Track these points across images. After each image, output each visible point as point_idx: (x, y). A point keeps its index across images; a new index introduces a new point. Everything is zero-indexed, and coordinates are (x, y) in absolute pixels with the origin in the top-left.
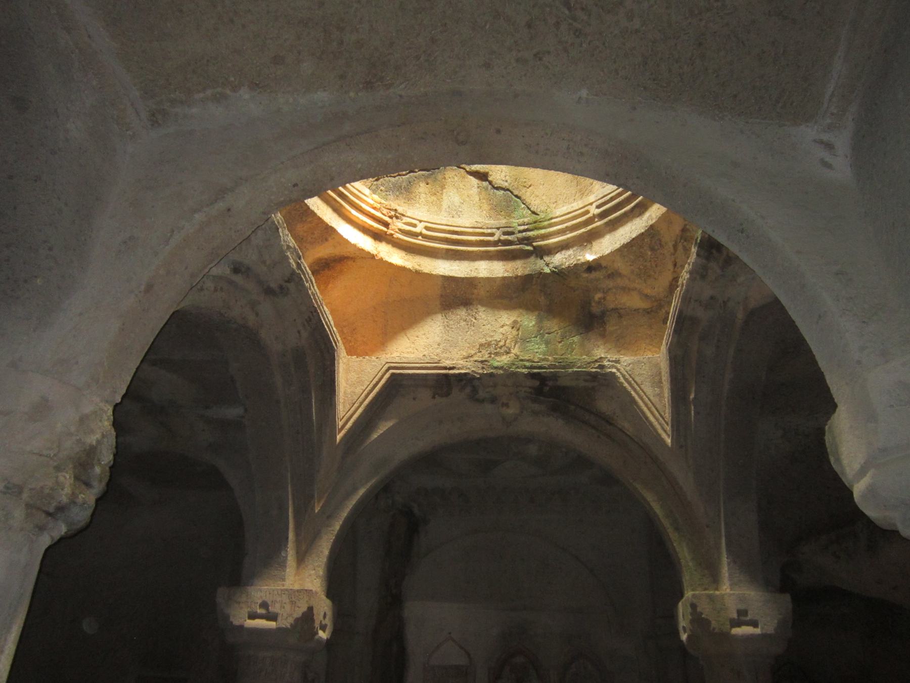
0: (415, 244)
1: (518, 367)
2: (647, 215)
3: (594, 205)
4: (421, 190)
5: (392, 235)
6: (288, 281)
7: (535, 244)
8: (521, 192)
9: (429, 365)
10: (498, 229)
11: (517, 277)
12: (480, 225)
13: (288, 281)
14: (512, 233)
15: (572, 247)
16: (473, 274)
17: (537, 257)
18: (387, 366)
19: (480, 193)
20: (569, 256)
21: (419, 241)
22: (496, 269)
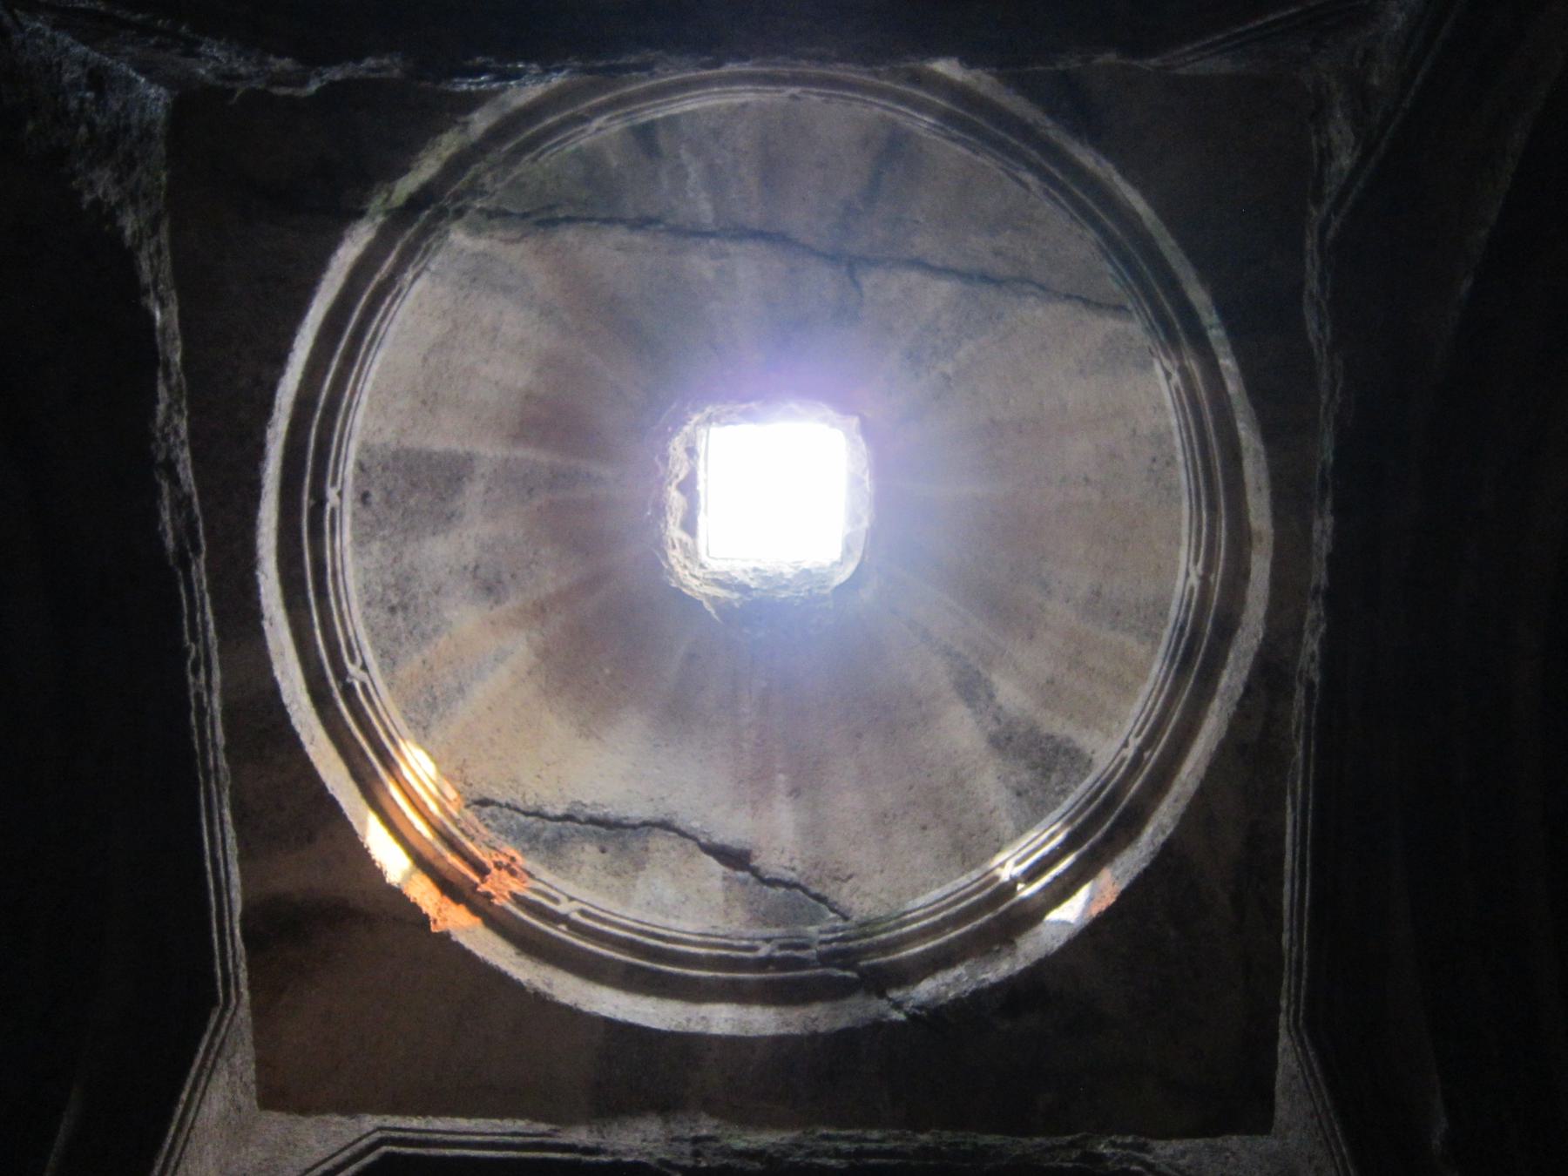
0: (547, 935)
1: (813, 1154)
2: (1149, 830)
3: (1010, 863)
4: (583, 857)
5: (488, 896)
7: (863, 963)
8: (830, 890)
9: (517, 1140)
10: (768, 940)
11: (814, 1036)
12: (721, 933)
14: (805, 947)
15: (962, 959)
16: (696, 1028)
17: (868, 992)
18: (378, 1135)
19: (728, 889)
20: (957, 979)
21: (560, 932)
22: (762, 1021)
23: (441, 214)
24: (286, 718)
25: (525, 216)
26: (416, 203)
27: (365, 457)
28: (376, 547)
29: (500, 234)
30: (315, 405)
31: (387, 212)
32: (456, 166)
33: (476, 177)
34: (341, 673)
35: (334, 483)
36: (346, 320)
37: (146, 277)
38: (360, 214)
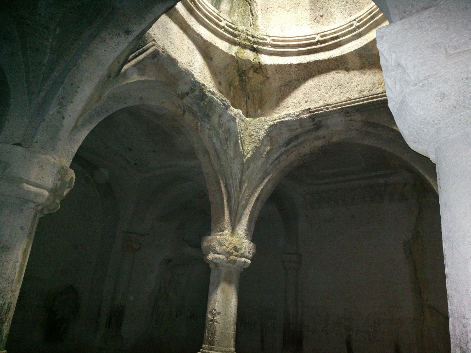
6: (313, 120)
13: (313, 120)
23: (254, 42)
24: (362, 47)
25: (249, 4)
26: (255, 50)
27: (313, 19)
28: (333, 10)
29: (256, 9)
30: (299, 51)
31: (258, 55)
32: (244, 47)
33: (245, 40)
34: (354, 30)
35: (314, 38)
36: (280, 52)
37: (272, 123)
38: (259, 63)
